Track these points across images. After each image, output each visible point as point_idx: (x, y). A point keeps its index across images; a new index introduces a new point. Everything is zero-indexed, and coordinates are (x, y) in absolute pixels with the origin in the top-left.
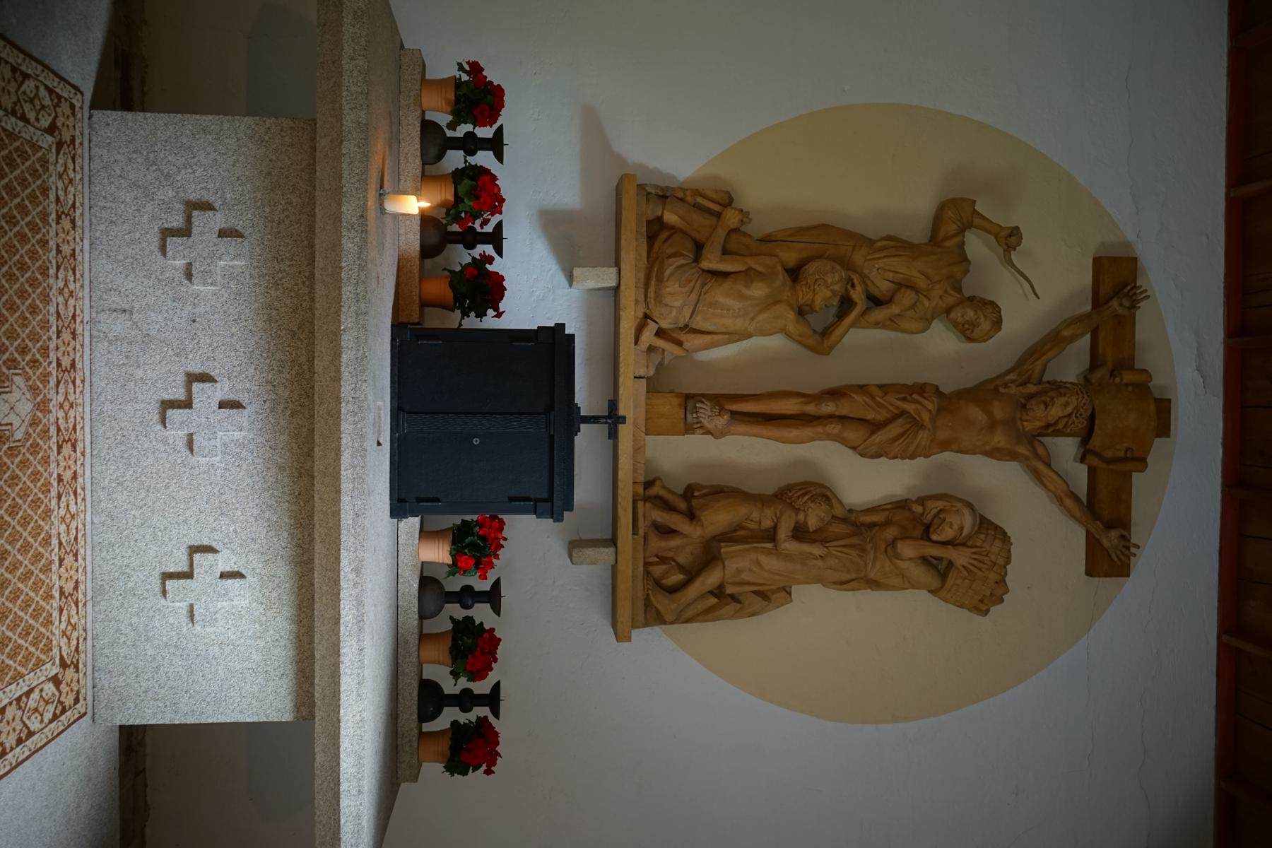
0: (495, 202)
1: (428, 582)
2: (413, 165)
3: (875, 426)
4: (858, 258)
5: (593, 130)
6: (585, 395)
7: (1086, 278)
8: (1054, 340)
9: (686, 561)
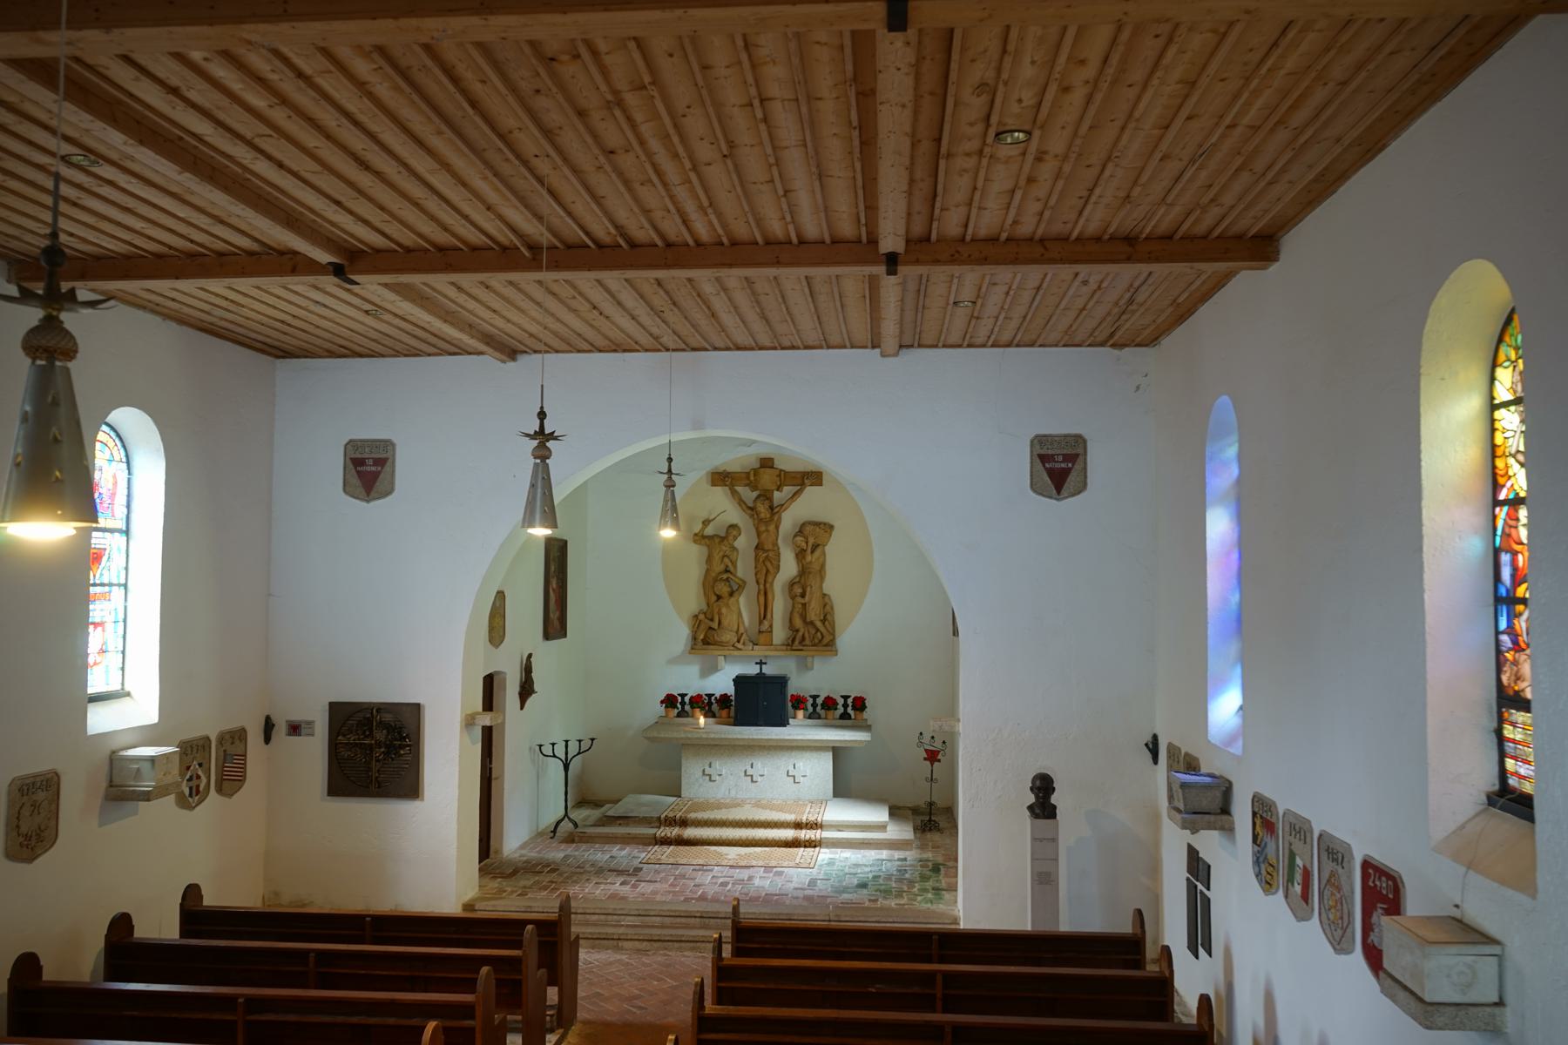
0: (699, 696)
2: (689, 720)
7: (718, 489)
8: (741, 502)
9: (813, 633)
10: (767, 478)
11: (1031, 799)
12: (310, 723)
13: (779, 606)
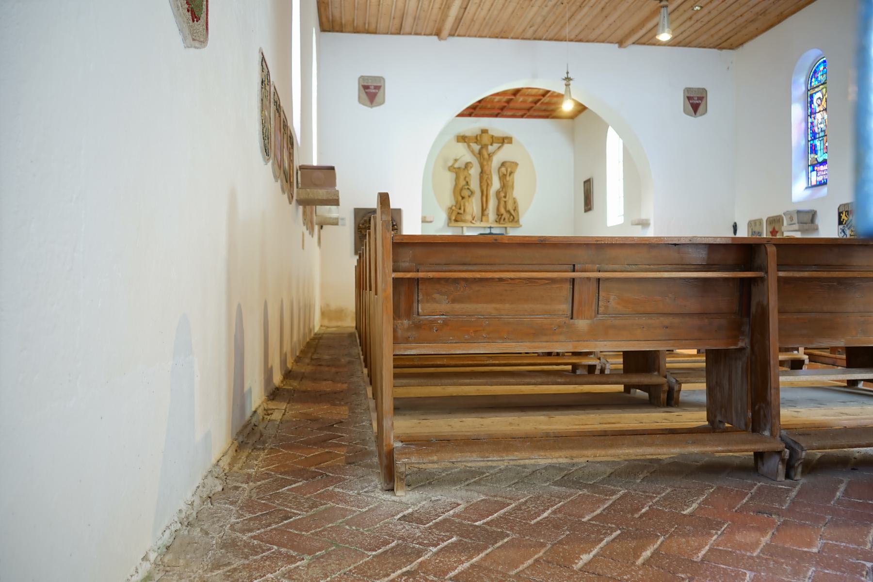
4: (460, 186)
6: (488, 231)
8: (473, 152)
10: (486, 139)
12: (343, 219)
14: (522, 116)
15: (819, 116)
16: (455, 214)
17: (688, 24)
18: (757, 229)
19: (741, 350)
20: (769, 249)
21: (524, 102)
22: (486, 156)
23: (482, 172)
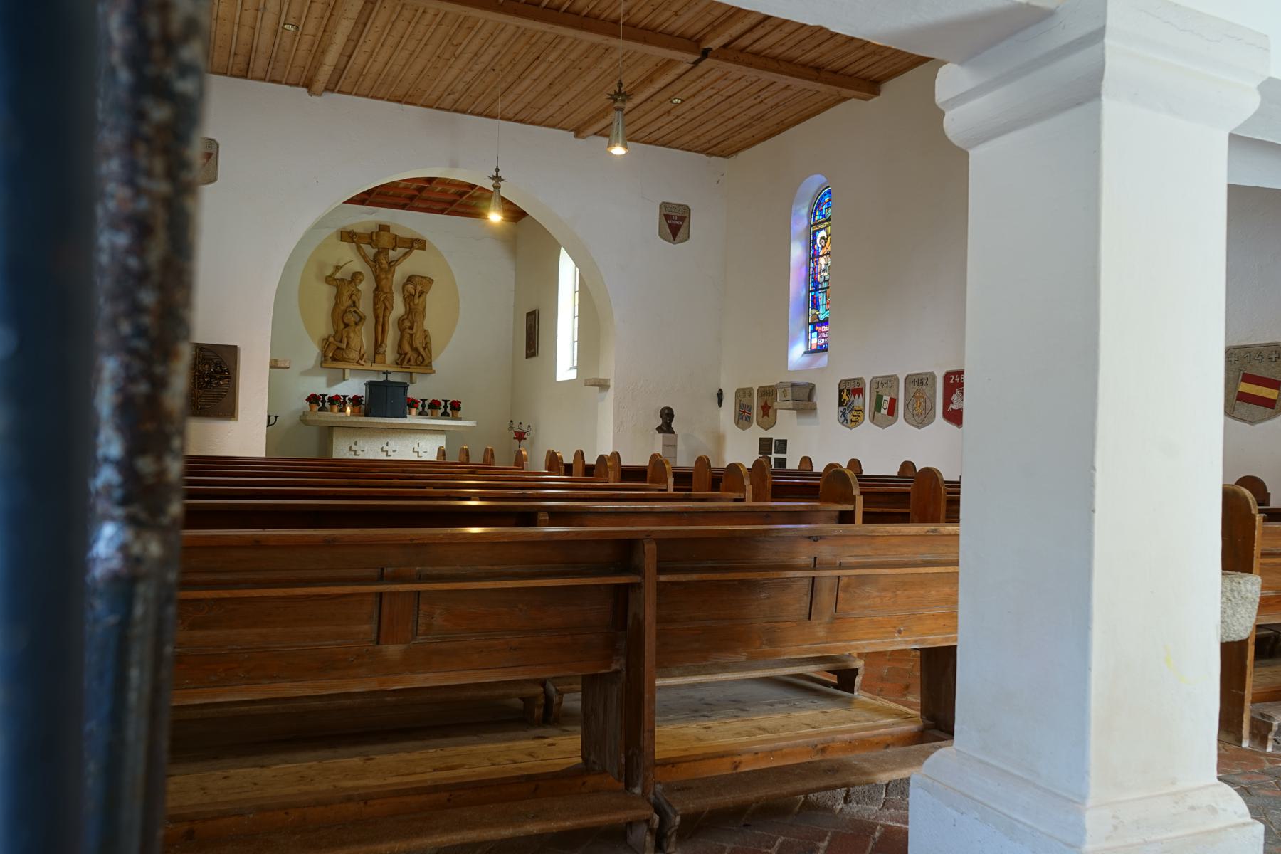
1: (420, 414)
3: (386, 308)
4: (343, 308)
5: (306, 373)
6: (382, 378)
7: (346, 244)
8: (364, 257)
9: (417, 355)
10: (385, 240)
11: (660, 422)
13: (391, 336)
14: (441, 212)
15: (822, 261)
16: (332, 347)
17: (666, 119)
18: (745, 401)
19: (617, 672)
20: (647, 546)
21: (443, 192)
22: (385, 266)
23: (378, 289)
